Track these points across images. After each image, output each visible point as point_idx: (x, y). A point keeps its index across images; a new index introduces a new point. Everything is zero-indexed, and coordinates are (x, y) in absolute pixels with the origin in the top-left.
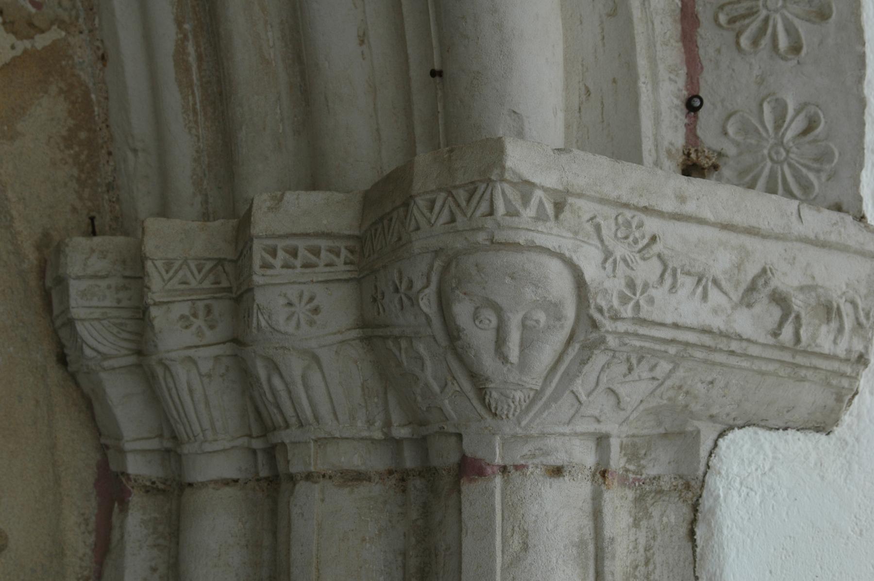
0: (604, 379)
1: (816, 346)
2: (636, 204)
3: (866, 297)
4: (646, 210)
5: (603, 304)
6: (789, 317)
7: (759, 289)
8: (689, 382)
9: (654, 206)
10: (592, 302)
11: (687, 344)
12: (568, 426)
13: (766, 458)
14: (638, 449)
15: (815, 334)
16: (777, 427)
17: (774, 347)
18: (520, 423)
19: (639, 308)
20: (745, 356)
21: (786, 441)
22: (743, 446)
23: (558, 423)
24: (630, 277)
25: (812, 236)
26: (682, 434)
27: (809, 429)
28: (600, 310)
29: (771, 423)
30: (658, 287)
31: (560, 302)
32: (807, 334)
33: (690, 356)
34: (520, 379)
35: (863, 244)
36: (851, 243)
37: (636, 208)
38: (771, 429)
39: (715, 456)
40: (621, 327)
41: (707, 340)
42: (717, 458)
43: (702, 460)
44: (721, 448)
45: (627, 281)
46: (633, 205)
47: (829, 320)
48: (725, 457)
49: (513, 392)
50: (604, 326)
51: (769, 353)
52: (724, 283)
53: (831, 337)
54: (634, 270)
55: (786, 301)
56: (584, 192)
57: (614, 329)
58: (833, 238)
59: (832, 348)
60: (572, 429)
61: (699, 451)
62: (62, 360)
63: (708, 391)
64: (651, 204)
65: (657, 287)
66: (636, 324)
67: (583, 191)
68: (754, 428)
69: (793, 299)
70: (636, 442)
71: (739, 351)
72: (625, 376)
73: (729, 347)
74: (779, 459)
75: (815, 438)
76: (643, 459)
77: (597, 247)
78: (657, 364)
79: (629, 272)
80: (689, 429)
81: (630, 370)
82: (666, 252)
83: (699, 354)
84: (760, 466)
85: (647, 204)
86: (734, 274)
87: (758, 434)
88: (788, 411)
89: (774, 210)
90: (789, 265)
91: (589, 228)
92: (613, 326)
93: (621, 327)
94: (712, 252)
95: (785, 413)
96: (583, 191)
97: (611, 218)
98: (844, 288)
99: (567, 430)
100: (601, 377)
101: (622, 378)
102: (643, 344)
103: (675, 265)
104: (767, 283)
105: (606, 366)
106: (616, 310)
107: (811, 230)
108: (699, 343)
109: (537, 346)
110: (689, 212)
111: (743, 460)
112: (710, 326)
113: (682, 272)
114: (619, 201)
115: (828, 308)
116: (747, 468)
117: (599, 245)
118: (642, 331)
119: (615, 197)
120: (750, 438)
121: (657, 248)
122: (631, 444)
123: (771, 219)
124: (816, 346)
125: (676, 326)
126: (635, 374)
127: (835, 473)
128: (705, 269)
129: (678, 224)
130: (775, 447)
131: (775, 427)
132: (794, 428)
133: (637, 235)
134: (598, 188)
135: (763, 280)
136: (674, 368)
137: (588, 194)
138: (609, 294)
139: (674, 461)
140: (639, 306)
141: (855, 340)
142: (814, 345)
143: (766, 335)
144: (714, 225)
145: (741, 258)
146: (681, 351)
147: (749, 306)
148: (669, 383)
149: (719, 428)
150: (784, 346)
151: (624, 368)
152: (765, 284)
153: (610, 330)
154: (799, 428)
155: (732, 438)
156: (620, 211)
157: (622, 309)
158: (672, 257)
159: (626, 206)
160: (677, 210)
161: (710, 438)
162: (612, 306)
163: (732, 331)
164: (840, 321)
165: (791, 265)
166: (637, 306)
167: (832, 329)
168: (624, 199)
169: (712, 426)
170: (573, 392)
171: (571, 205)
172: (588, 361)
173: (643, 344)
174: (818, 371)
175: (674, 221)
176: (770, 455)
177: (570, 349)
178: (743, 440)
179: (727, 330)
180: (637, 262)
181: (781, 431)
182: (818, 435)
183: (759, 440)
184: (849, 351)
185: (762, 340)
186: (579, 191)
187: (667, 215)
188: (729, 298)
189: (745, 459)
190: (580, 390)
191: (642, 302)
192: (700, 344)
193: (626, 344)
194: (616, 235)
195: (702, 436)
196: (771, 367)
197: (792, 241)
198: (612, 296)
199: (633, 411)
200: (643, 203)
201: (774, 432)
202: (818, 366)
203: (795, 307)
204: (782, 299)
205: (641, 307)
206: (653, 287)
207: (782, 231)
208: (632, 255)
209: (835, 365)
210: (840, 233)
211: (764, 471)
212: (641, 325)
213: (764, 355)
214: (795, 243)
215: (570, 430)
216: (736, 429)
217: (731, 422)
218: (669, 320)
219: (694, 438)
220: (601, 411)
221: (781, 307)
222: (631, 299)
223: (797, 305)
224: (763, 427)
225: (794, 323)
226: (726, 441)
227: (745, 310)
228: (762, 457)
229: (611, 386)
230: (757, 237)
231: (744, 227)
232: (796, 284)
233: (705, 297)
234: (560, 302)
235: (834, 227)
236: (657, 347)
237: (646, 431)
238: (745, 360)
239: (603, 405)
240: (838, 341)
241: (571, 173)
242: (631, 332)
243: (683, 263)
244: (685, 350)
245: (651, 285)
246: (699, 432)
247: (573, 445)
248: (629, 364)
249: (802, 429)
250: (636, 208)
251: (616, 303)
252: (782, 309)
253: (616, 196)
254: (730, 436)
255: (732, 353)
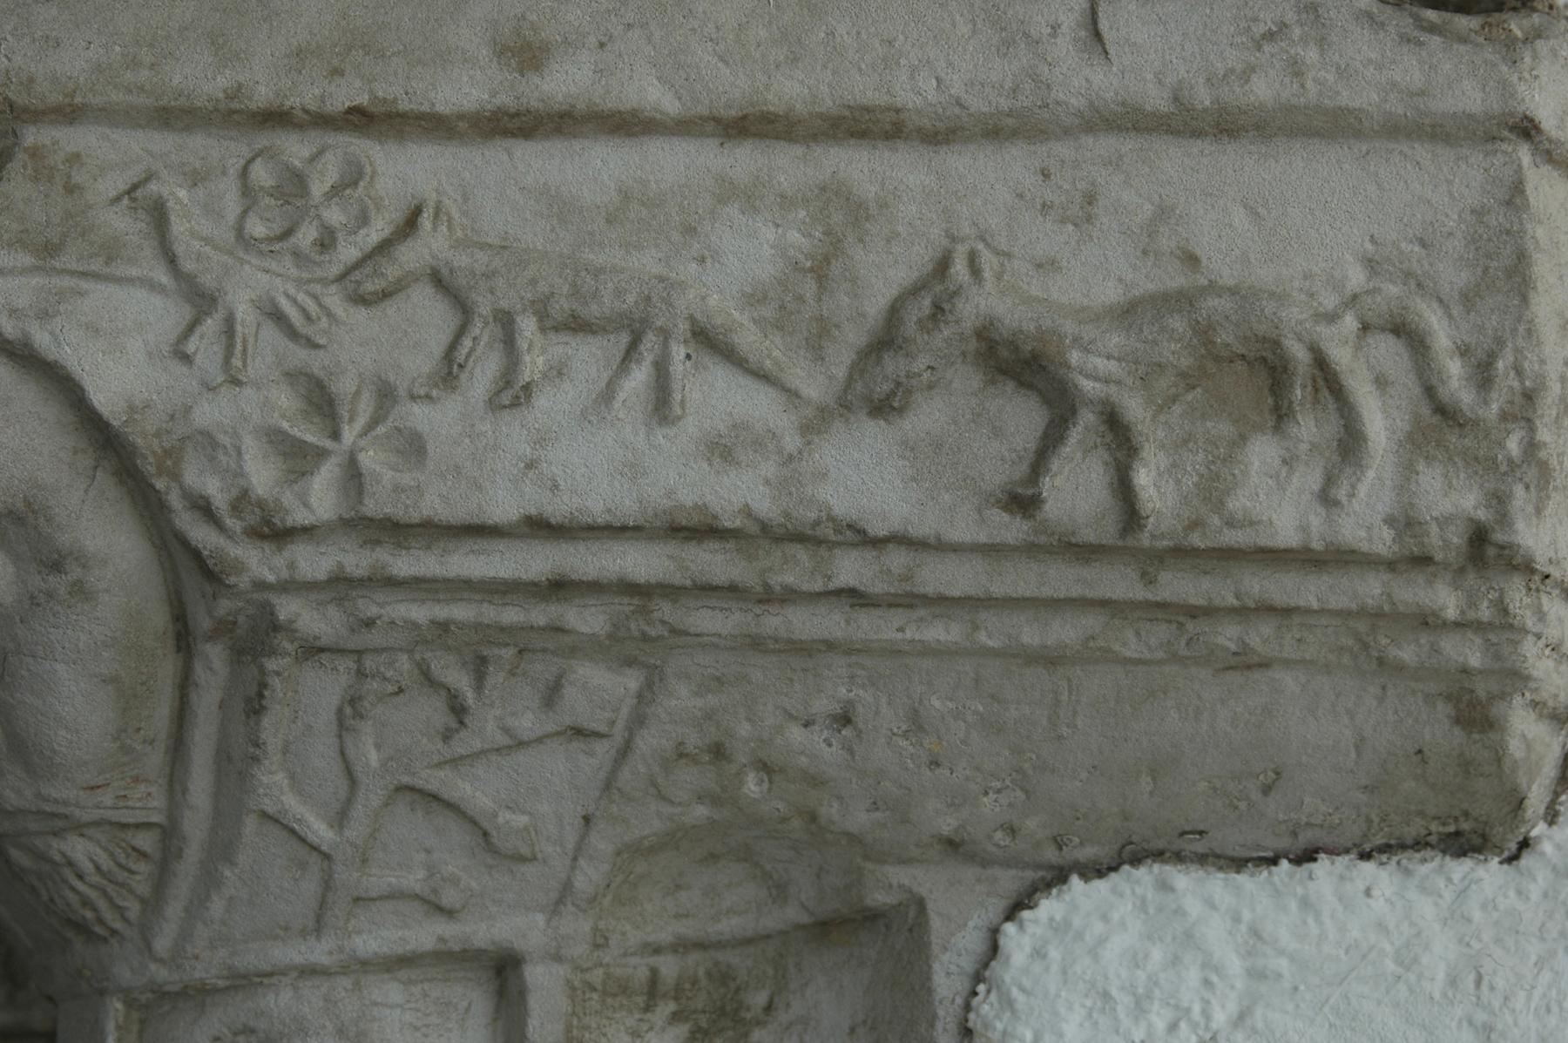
0: (370, 756)
1: (1231, 523)
2: (313, 107)
3: (1468, 299)
4: (361, 119)
5: (214, 489)
6: (1068, 428)
7: (905, 340)
8: (744, 730)
9: (396, 99)
10: (168, 488)
11: (629, 588)
12: (318, 938)
13: (1214, 978)
14: (738, 990)
15: (1217, 477)
16: (1269, 854)
17: (1030, 550)
18: (149, 947)
19: (361, 485)
20: (909, 601)
21: (1305, 903)
22: (1102, 941)
23: (282, 933)
24: (310, 377)
25: (1157, 100)
26: (872, 918)
27: (1419, 845)
28: (204, 509)
29: (1232, 840)
30: (434, 393)
31: (28, 504)
32: (1178, 482)
33: (675, 631)
34: (38, 795)
35: (1422, 93)
36: (1363, 97)
37: (323, 121)
38: (1239, 864)
39: (989, 991)
40: (313, 562)
41: (714, 563)
42: (993, 996)
43: (941, 1013)
44: (1008, 958)
45: (303, 391)
46: (306, 111)
47: (1281, 416)
48: (1023, 989)
49: (56, 844)
50: (239, 567)
51: (1021, 579)
52: (748, 339)
53: (1309, 478)
54: (316, 346)
55: (1044, 368)
56: (78, 100)
57: (285, 574)
58: (1264, 90)
59: (1316, 521)
60: (341, 950)
61: (927, 977)
62: (485, 834)
63: (851, 751)
64: (380, 94)
65: (428, 397)
66: (378, 542)
67: (72, 95)
68: (1156, 867)
69: (1075, 357)
70: (729, 966)
71: (878, 588)
72: (447, 736)
73: (830, 578)
74: (1279, 976)
75: (1449, 880)
76: (759, 1023)
77: (152, 286)
78: (560, 677)
79: (299, 355)
80: (878, 898)
81: (458, 710)
82: (462, 260)
83: (708, 620)
84: (1188, 1010)
85: (363, 100)
86: (800, 299)
87: (1172, 890)
88: (1266, 790)
89: (965, 30)
90: (1071, 227)
91: (122, 224)
92: (279, 561)
93: (313, 562)
94: (690, 231)
95: (1255, 795)
96: (72, 95)
97: (224, 173)
98: (1356, 278)
99: (319, 952)
100: (351, 753)
101: (440, 745)
102: (442, 612)
103: (504, 304)
104: (943, 310)
105: (348, 710)
106: (261, 504)
107: (1149, 77)
108: (677, 579)
109: (24, 673)
110: (560, 97)
111: (1106, 996)
112: (702, 508)
113: (549, 324)
114: (235, 105)
115: (1272, 370)
116: (1126, 1022)
117: (162, 276)
118: (404, 564)
119: (221, 95)
120: (1142, 906)
121: (430, 246)
122: (709, 974)
123: (950, 64)
124: (1231, 523)
125: (539, 527)
126: (486, 726)
127: (1548, 1010)
128: (648, 298)
129: (525, 151)
130: (1255, 933)
131: (1255, 855)
132: (1347, 851)
133: (335, 216)
134: (145, 74)
135: (927, 302)
136: (649, 685)
137: (97, 101)
138: (225, 447)
139: (864, 1022)
140: (361, 475)
141: (1430, 479)
142: (1216, 520)
143: (980, 512)
144: (684, 127)
145: (827, 233)
146: (627, 618)
147: (884, 408)
148: (650, 741)
149: (1010, 881)
150: (1073, 541)
151: (432, 710)
152: (933, 317)
153: (271, 578)
154: (1367, 847)
155: (1058, 917)
156: (263, 140)
157: (288, 499)
158: (489, 275)
159: (276, 118)
160: (505, 100)
161: (971, 924)
162: (245, 494)
163: (812, 515)
164: (1340, 410)
165: (1076, 225)
166: (353, 476)
167: (1304, 447)
168: (262, 95)
169: (979, 880)
170: (264, 815)
171: (35, 153)
172: (264, 702)
173: (442, 612)
174: (1296, 619)
175: (510, 142)
176: (1235, 965)
177: (198, 668)
178: (1105, 918)
179: (787, 515)
180: (330, 315)
181: (1284, 864)
182: (1460, 868)
183: (1180, 912)
184: (1406, 523)
185: (963, 530)
186: (55, 98)
187: (462, 125)
188: (785, 389)
189: (1114, 992)
190: (293, 804)
191: (369, 459)
192: (688, 583)
193: (369, 623)
194: (240, 230)
195: (936, 923)
196: (1065, 631)
197: (1067, 132)
198: (239, 453)
199: (575, 859)
200: (346, 94)
201: (1252, 875)
202: (1279, 598)
203: (1087, 385)
204: (1026, 362)
205: (367, 480)
206: (413, 398)
207: (1005, 104)
208: (308, 293)
209: (1371, 588)
210: (1296, 69)
211: (1207, 1028)
212: (399, 545)
213: (997, 590)
214: (1089, 140)
215: (331, 953)
216: (1075, 880)
217: (1050, 854)
218: (504, 506)
219: (910, 930)
220: (431, 870)
221: (1040, 392)
222: (322, 454)
223: (1096, 379)
224: (1202, 859)
225: (1108, 447)
226: (1031, 928)
227: (872, 431)
228: (1193, 975)
229: (406, 779)
230: (900, 144)
231: (821, 116)
232: (1109, 293)
233: (662, 404)
234: (28, 504)
235: (1266, 48)
236: (511, 615)
237: (735, 921)
238: (935, 616)
239: (428, 851)
240: (1341, 493)
241: (27, 40)
242: (360, 573)
243: (543, 287)
244: (644, 611)
245: (402, 392)
246: (921, 904)
247: (376, 1004)
248: (443, 693)
249: (1386, 849)
250: (323, 121)
251: (262, 475)
252: (1047, 402)
253: (225, 91)
254: (1048, 908)
255: (855, 597)
